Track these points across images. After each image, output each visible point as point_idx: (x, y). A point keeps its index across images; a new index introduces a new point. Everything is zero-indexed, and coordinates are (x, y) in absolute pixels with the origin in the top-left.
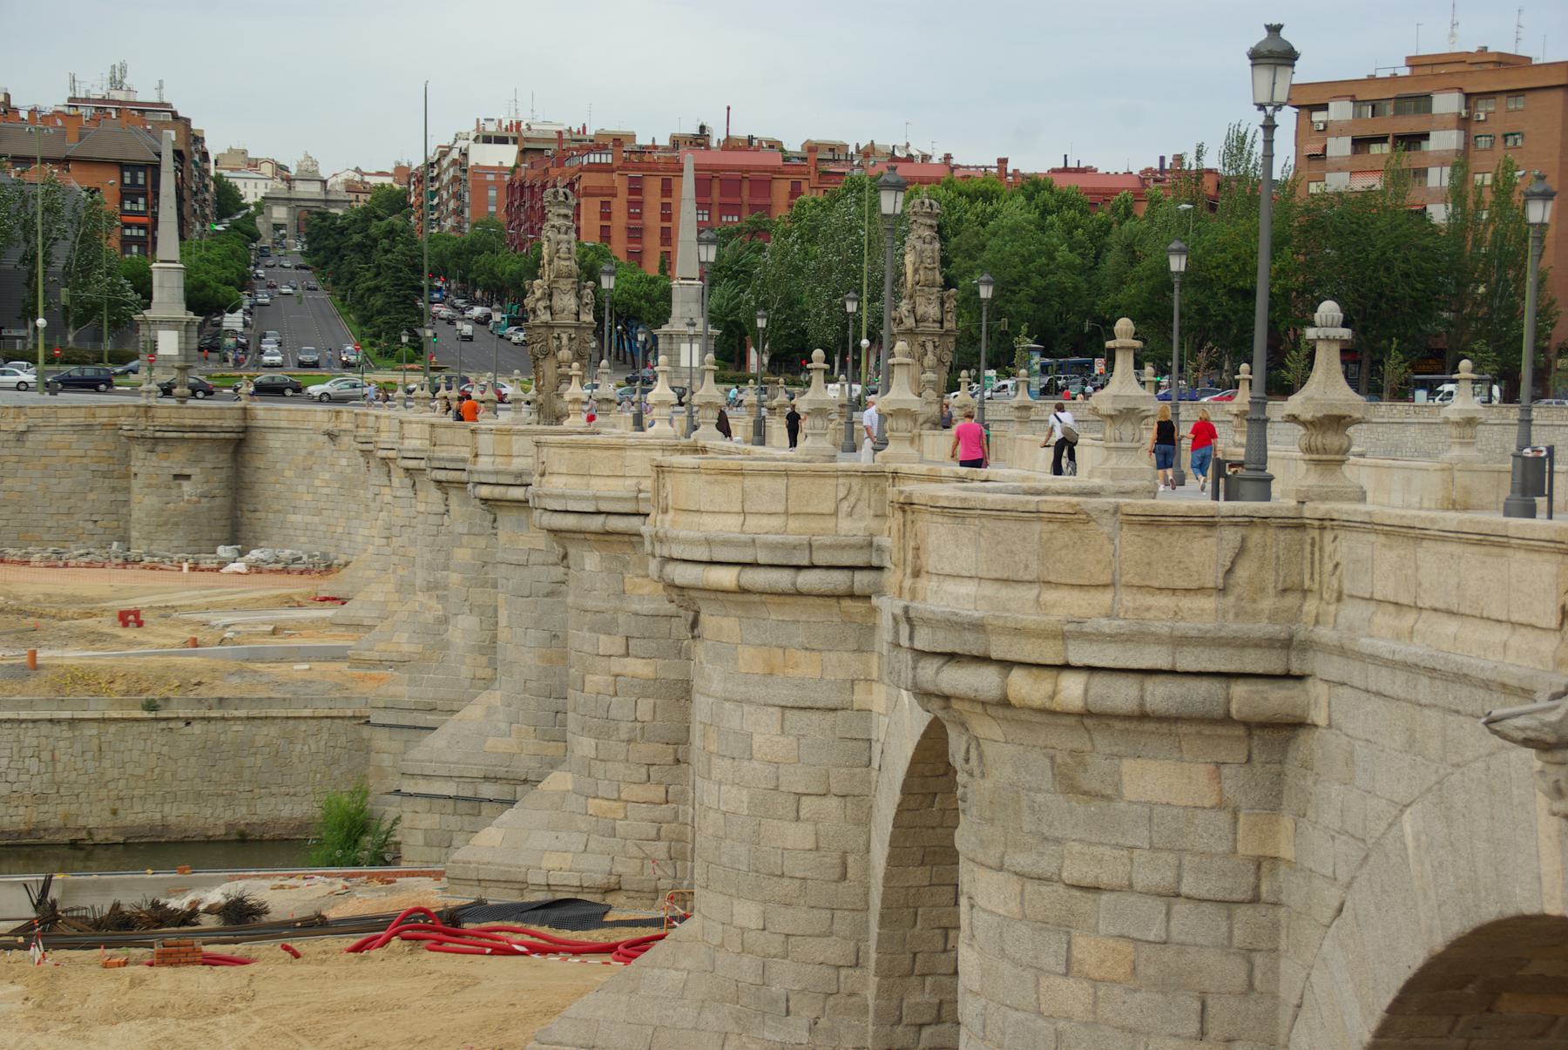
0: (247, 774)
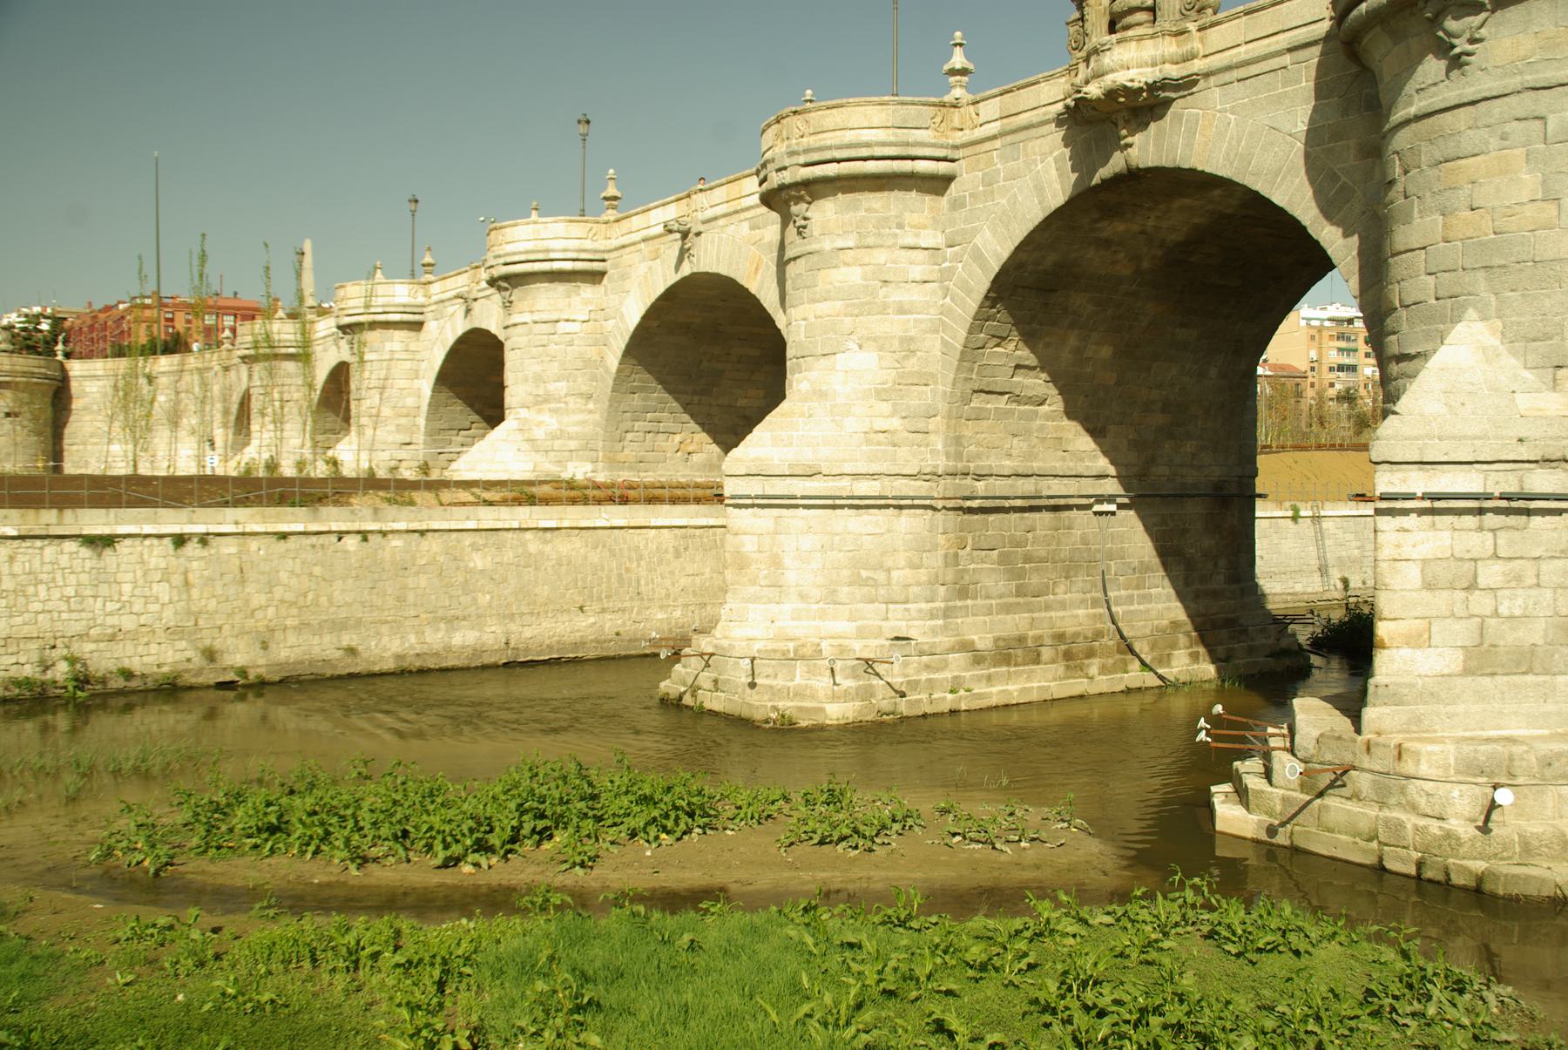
0: (411, 597)
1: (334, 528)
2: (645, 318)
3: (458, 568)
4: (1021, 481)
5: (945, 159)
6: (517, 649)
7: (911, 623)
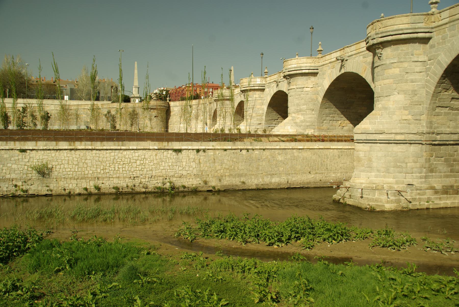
0: (260, 168)
1: (239, 148)
2: (330, 86)
3: (274, 160)
4: (453, 136)
5: (428, 32)
6: (291, 184)
7: (413, 180)
